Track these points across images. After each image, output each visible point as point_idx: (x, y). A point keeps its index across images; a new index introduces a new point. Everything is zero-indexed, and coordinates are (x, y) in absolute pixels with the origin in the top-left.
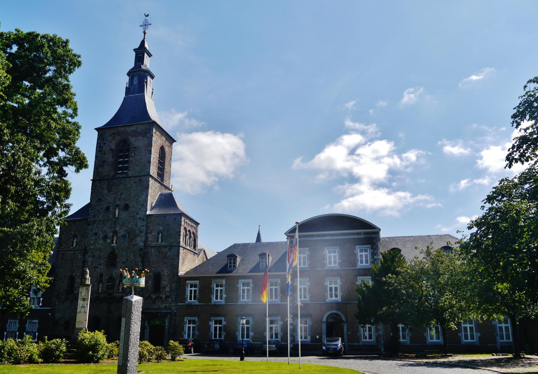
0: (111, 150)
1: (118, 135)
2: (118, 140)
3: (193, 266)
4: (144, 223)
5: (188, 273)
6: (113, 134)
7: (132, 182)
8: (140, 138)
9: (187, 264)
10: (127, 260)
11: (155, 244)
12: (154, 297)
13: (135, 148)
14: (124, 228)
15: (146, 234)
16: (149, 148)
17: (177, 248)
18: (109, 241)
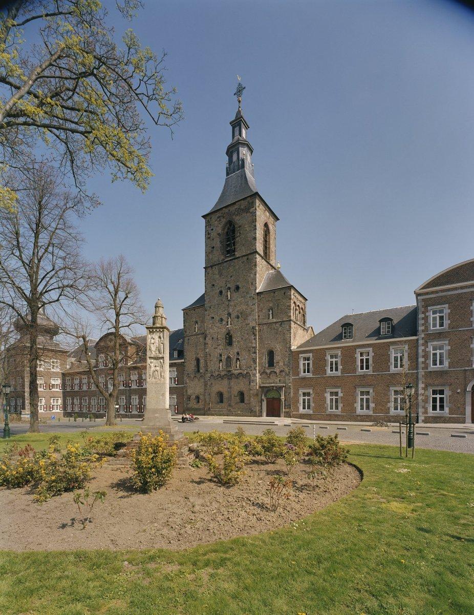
0: (219, 234)
1: (224, 217)
2: (223, 223)
5: (300, 346)
6: (218, 218)
8: (244, 214)
11: (265, 321)
12: (268, 371)
13: (240, 227)
16: (254, 224)
18: (224, 323)
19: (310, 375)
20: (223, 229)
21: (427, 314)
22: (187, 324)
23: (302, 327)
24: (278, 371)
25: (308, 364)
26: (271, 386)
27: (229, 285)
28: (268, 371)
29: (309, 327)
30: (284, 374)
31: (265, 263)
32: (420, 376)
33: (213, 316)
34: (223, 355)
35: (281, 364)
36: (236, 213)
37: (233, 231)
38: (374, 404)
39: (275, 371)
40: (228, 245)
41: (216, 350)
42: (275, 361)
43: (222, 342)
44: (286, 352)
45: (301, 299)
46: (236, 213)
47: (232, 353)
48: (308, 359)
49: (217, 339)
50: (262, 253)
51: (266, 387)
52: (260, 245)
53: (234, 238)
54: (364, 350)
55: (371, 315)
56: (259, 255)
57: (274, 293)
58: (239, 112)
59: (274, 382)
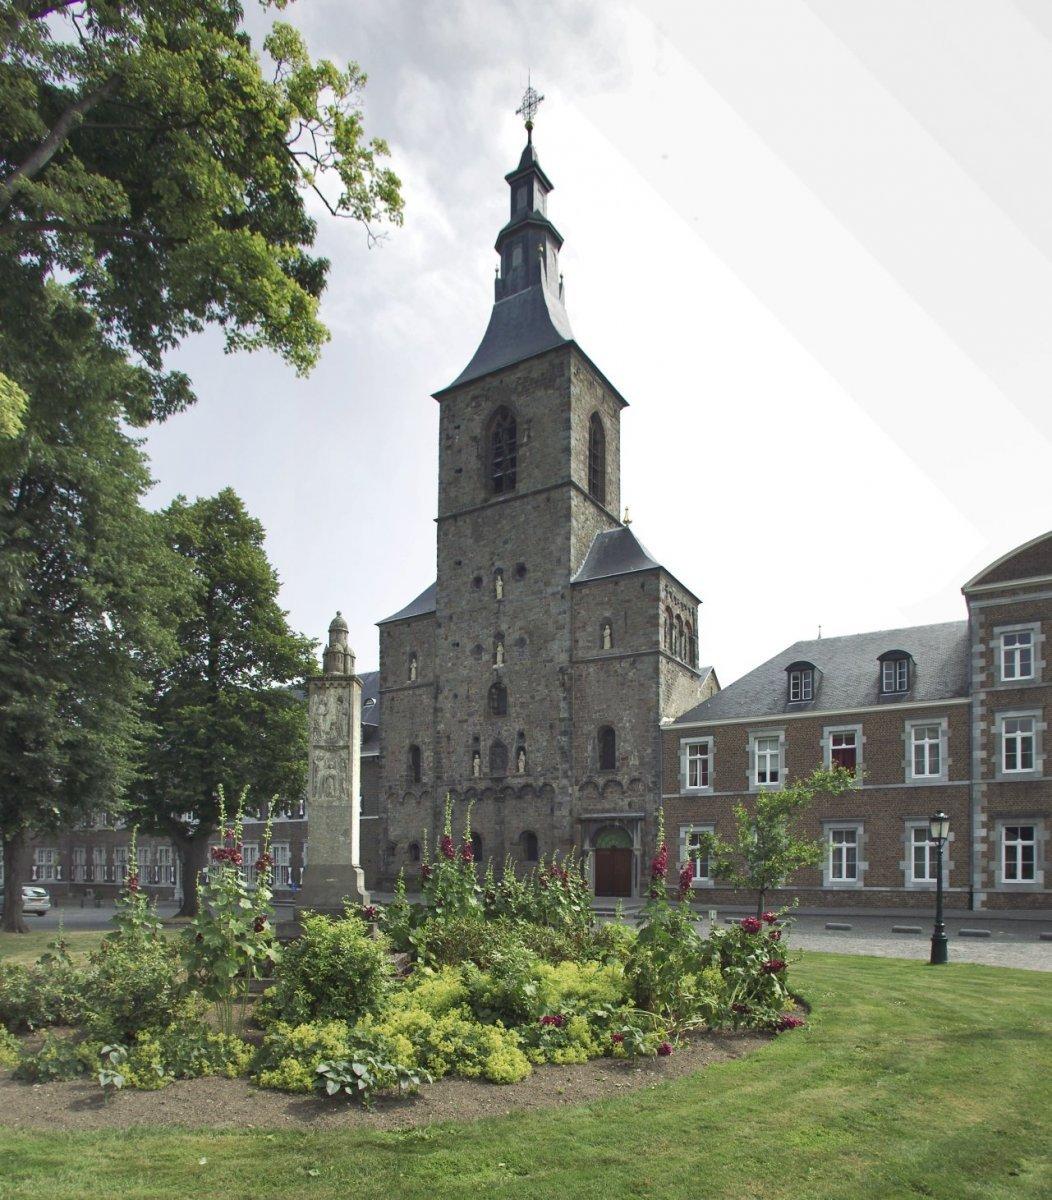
0: (474, 439)
1: (487, 399)
3: (691, 704)
4: (566, 605)
6: (474, 398)
7: (529, 507)
8: (540, 393)
9: (676, 702)
10: (533, 697)
11: (593, 654)
12: (601, 781)
14: (519, 624)
15: (572, 632)
17: (652, 659)
18: (486, 657)
19: (707, 790)
20: (487, 426)
21: (992, 644)
22: (388, 661)
23: (688, 669)
24: (625, 781)
25: (705, 762)
26: (607, 819)
27: (498, 564)
28: (601, 781)
29: (706, 670)
30: (641, 787)
31: (591, 510)
32: (977, 795)
33: (458, 640)
34: (482, 738)
35: (634, 761)
36: (520, 389)
37: (512, 432)
38: (867, 863)
39: (619, 778)
40: (498, 465)
42: (617, 754)
43: (480, 705)
44: (647, 731)
45: (685, 600)
46: (520, 389)
47: (509, 729)
48: (703, 749)
49: (468, 697)
50: (584, 486)
51: (595, 820)
52: (581, 466)
53: (513, 448)
54: (842, 728)
55: (860, 642)
56: (578, 489)
57: (616, 583)
58: (528, 152)
59: (617, 805)
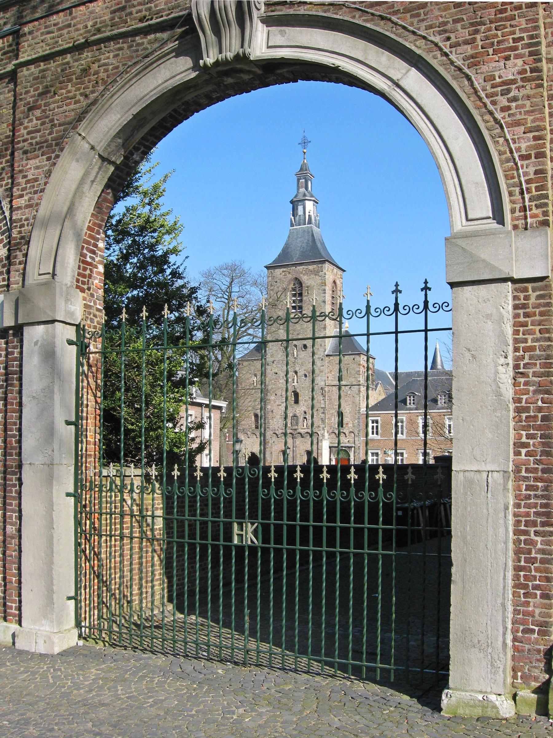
14: (304, 368)
35: (350, 425)
41: (280, 407)
